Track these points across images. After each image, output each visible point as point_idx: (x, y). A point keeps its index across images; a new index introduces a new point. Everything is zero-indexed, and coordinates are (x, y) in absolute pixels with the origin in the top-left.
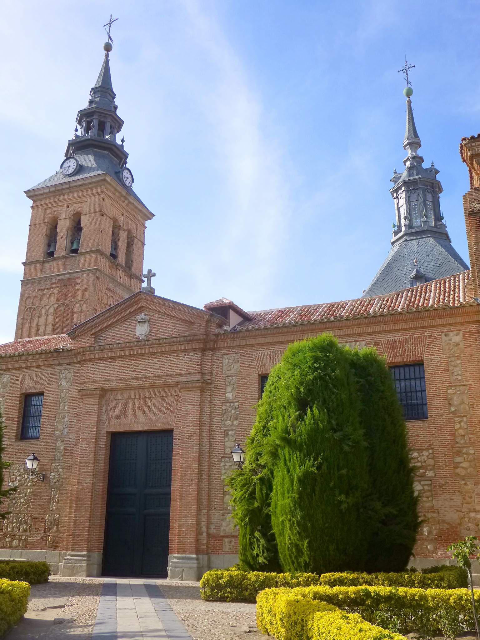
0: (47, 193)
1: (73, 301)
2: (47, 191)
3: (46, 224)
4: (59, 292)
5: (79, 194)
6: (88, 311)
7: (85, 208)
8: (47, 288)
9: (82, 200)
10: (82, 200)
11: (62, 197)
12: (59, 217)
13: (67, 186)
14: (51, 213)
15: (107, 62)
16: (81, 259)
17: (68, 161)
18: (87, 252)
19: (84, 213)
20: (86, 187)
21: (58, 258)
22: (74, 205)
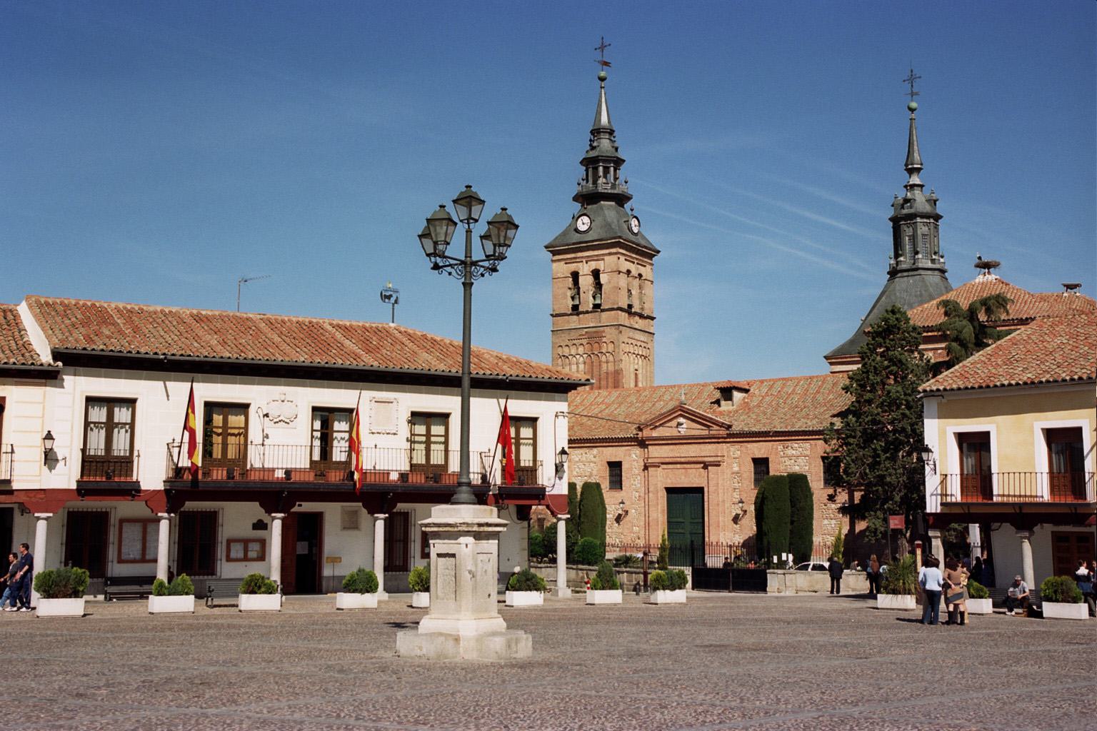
16: (604, 315)
19: (602, 269)
22: (592, 262)
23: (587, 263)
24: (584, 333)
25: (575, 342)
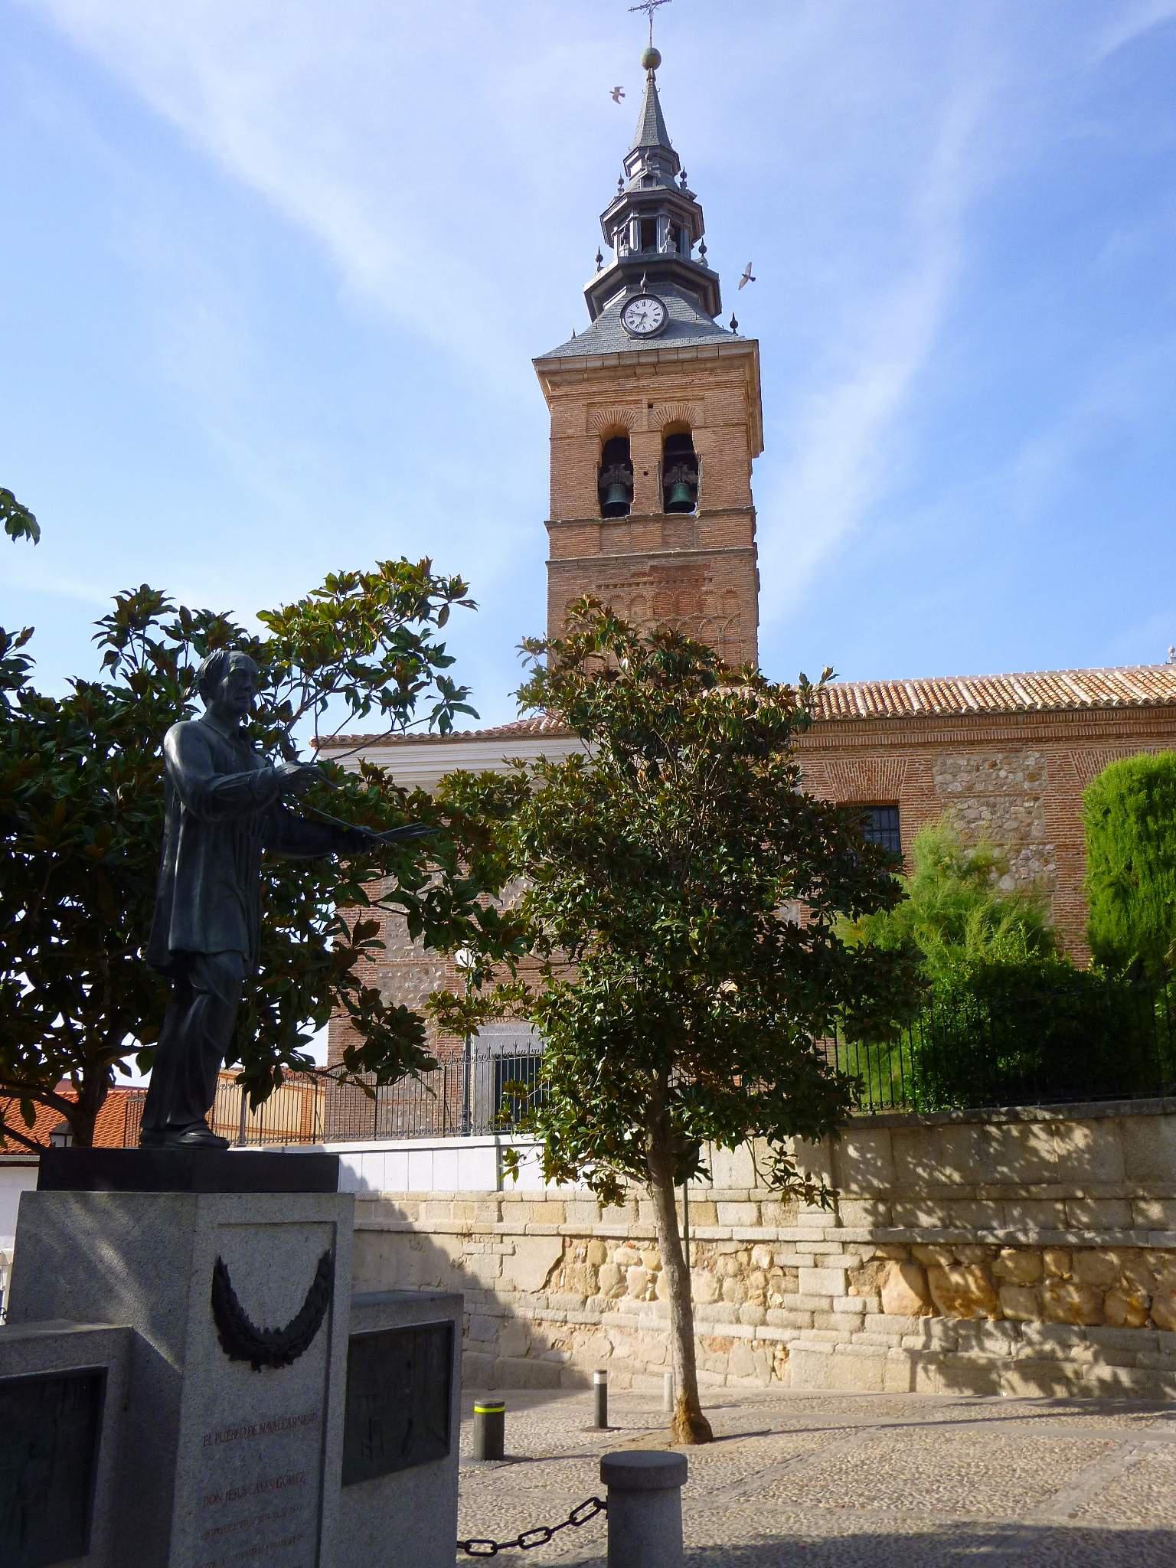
0: (595, 370)
1: (698, 618)
2: (598, 364)
3: (597, 440)
4: (659, 594)
5: (679, 380)
6: (743, 641)
7: (696, 413)
8: (623, 585)
9: (689, 394)
10: (689, 394)
11: (632, 382)
12: (629, 426)
13: (653, 359)
14: (608, 415)
15: (653, 93)
17: (640, 303)
18: (724, 510)
20: (697, 366)
21: (643, 519)
22: (669, 404)
23: (650, 406)
24: (647, 568)
25: (619, 591)
